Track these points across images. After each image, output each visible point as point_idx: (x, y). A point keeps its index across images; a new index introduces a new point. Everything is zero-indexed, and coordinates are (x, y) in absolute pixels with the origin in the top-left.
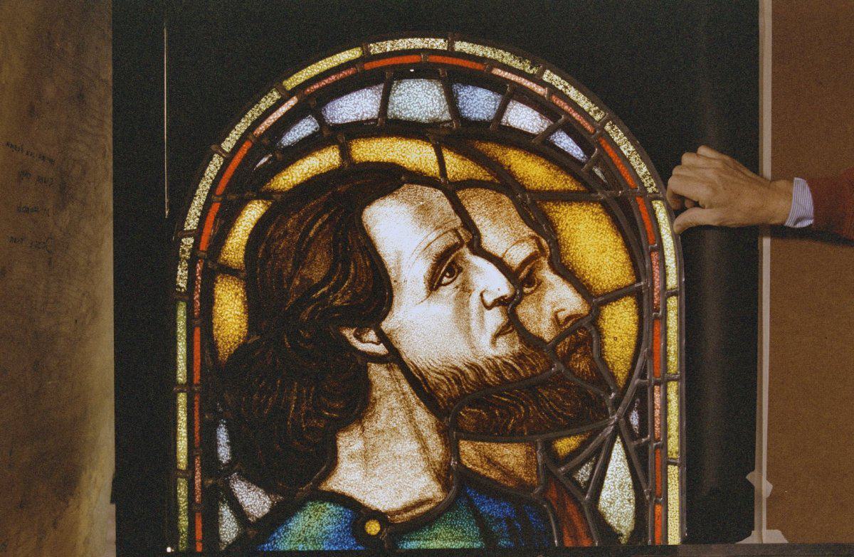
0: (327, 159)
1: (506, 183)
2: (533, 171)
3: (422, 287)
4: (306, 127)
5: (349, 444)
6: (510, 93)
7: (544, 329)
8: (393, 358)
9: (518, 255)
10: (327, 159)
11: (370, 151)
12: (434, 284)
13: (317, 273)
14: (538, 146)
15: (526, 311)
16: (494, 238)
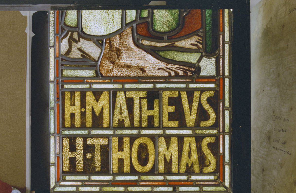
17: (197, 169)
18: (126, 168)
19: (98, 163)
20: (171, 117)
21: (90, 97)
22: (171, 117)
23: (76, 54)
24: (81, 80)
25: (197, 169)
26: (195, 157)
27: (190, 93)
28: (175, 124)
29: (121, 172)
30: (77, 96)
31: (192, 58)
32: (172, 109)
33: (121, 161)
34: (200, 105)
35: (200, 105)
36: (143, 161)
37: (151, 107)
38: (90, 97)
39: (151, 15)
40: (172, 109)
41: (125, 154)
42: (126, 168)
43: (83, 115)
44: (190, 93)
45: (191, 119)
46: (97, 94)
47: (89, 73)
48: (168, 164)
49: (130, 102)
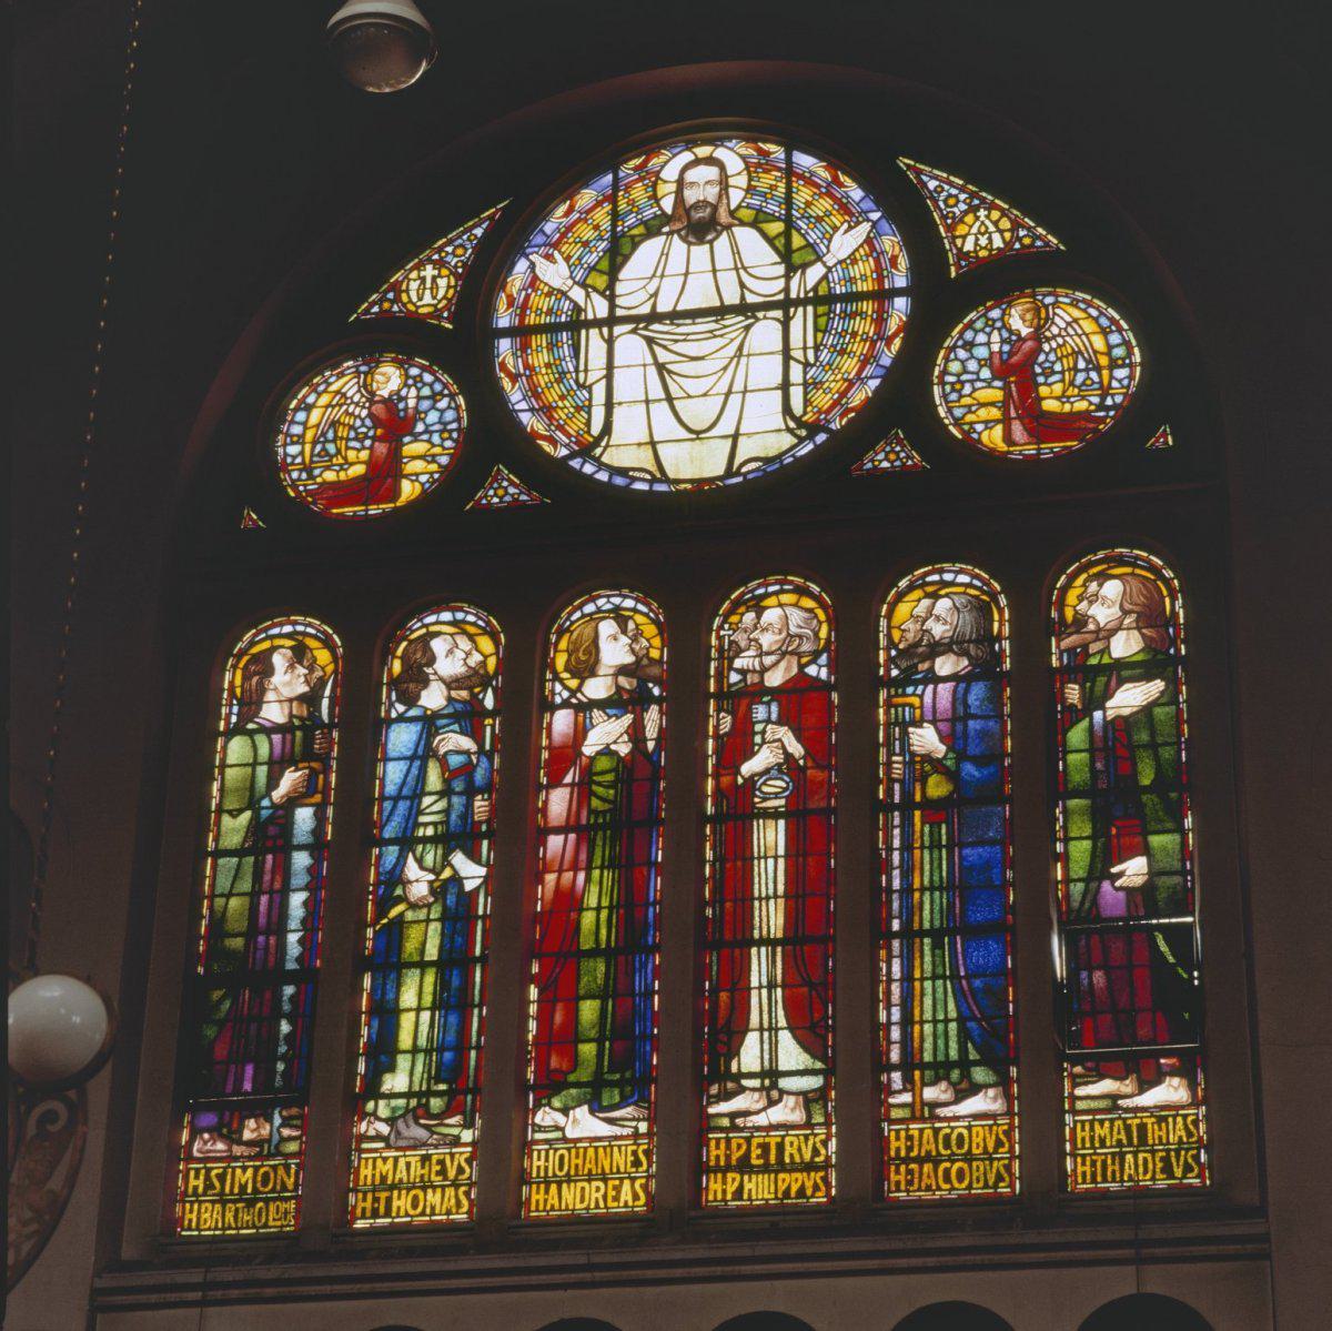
0: (424, 631)
1: (465, 632)
2: (471, 630)
3: (443, 657)
4: (419, 624)
5: (424, 693)
6: (467, 613)
7: (473, 665)
8: (436, 673)
9: (467, 649)
10: (424, 631)
11: (432, 629)
12: (447, 656)
13: (418, 655)
14: (474, 624)
15: (468, 661)
16: (461, 645)
17: (454, 1210)
18: (402, 1213)
19: (382, 1210)
20: (438, 1173)
21: (379, 1162)
22: (438, 1173)
23: (372, 1133)
24: (375, 1150)
25: (454, 1210)
26: (453, 1201)
27: (452, 1155)
28: (440, 1178)
29: (398, 1216)
30: (370, 1161)
31: (455, 1131)
32: (438, 1168)
33: (399, 1208)
34: (459, 1165)
35: (459, 1165)
36: (415, 1206)
37: (423, 1167)
38: (379, 1162)
39: (428, 1101)
40: (438, 1168)
41: (401, 1203)
42: (402, 1213)
43: (374, 1176)
44: (452, 1155)
45: (452, 1173)
46: (385, 1160)
47: (381, 1145)
48: (433, 1208)
49: (408, 1165)
